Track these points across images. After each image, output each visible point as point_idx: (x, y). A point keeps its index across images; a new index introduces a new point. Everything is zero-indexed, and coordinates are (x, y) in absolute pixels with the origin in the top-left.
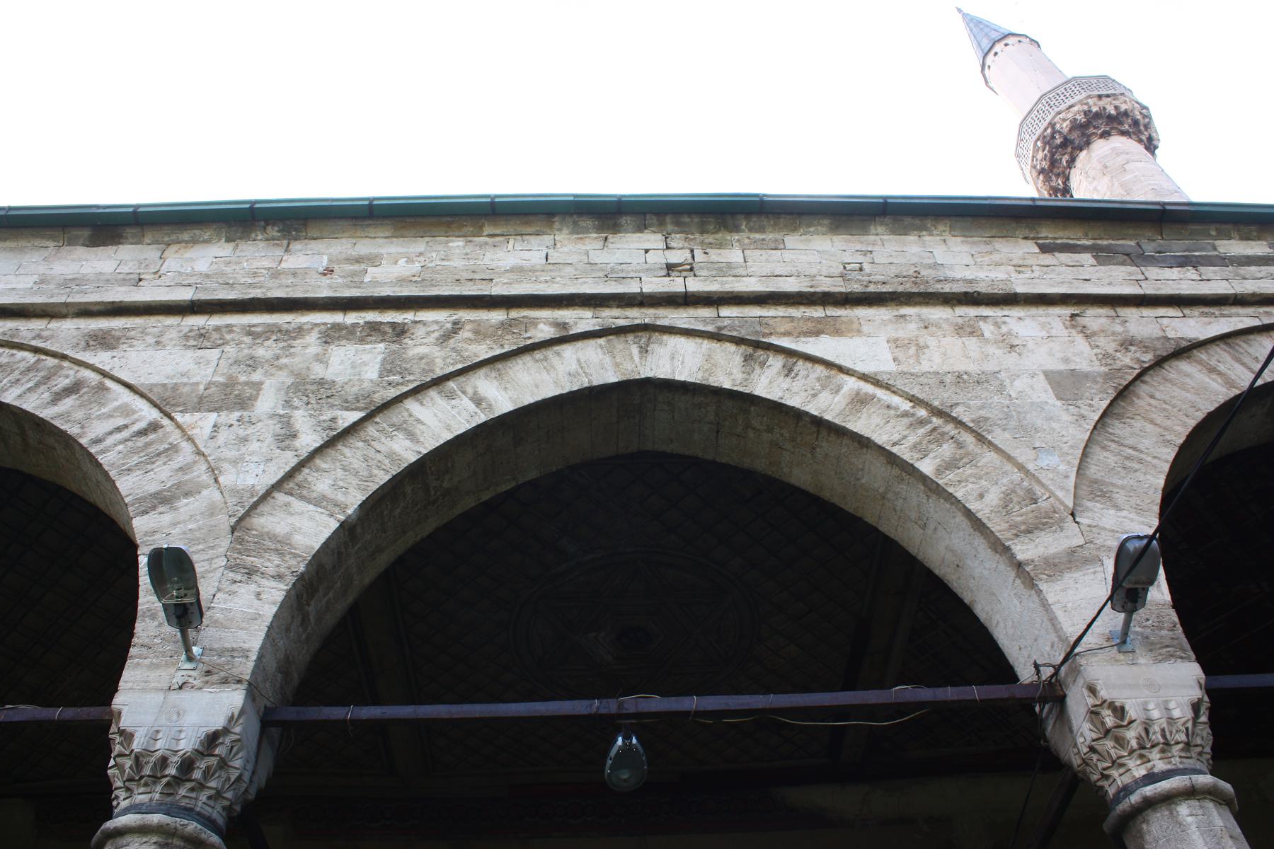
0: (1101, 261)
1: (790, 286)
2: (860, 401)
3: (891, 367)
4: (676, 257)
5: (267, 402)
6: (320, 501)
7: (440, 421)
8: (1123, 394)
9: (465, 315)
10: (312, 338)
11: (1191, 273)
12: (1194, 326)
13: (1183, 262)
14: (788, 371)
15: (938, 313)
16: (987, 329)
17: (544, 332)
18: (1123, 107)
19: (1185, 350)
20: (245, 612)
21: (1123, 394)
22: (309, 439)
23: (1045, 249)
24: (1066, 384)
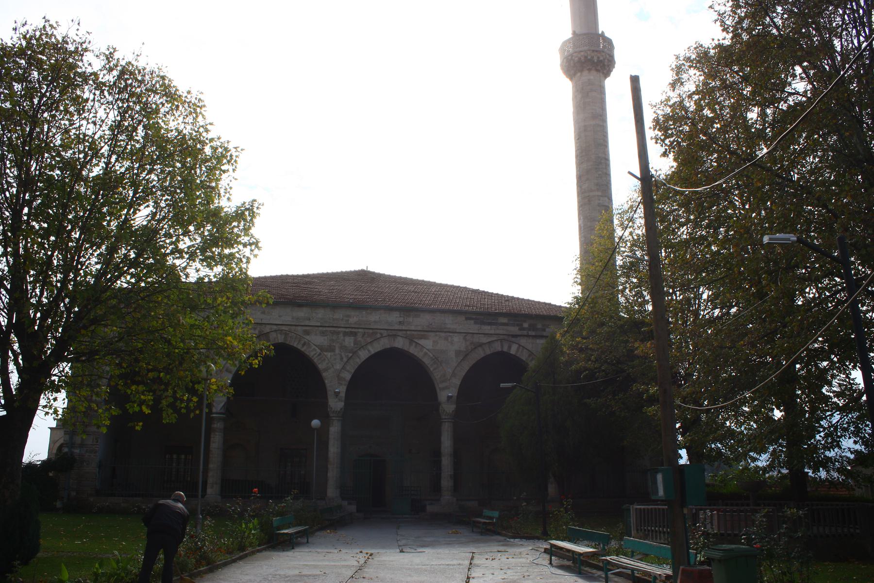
0: (475, 323)
1: (419, 328)
2: (426, 354)
3: (431, 347)
4: (401, 319)
5: (337, 351)
6: (348, 371)
7: (364, 355)
8: (466, 356)
9: (366, 331)
10: (341, 335)
11: (489, 327)
12: (485, 340)
13: (490, 324)
14: (416, 347)
15: (443, 334)
16: (450, 339)
17: (379, 336)
18: (601, 58)
19: (481, 345)
20: (342, 389)
21: (466, 356)
22: (345, 360)
23: (467, 319)
24: (458, 353)
